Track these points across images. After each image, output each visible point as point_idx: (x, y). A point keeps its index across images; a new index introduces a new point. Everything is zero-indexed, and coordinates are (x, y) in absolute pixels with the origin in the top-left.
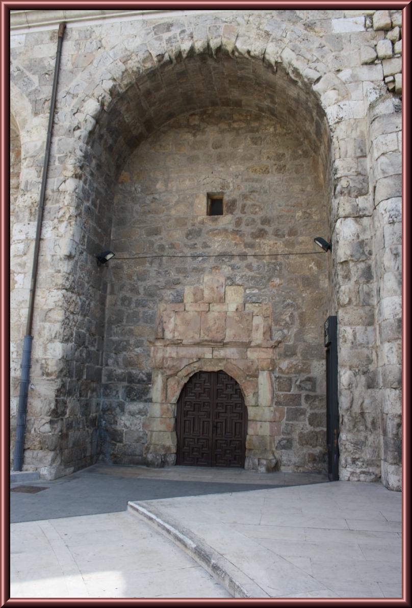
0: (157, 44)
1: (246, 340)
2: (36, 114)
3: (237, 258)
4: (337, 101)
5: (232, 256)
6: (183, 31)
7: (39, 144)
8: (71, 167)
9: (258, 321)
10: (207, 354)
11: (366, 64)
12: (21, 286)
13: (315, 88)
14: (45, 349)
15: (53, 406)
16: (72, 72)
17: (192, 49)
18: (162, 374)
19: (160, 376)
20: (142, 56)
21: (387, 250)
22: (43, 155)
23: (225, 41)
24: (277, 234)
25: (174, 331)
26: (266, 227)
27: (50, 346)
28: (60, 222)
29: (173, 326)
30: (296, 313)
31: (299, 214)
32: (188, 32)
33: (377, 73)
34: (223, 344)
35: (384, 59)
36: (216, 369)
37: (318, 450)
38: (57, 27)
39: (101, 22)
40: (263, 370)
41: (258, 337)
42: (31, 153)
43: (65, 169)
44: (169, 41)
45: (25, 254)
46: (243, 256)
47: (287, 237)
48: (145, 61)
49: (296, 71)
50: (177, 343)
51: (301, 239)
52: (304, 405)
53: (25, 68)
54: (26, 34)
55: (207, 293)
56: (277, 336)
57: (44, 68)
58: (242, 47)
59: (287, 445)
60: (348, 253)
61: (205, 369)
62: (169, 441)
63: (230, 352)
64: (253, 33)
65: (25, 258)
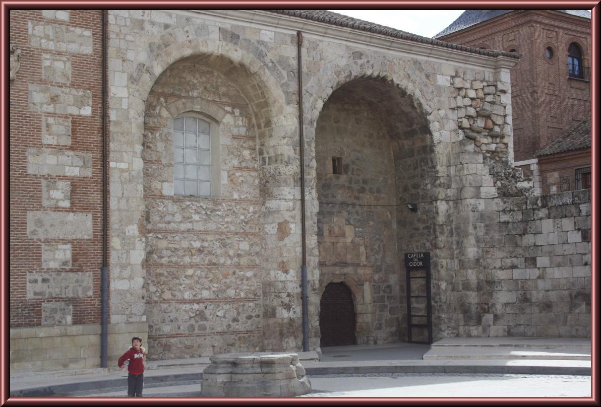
0: (355, 67)
2: (288, 104)
3: (351, 206)
5: (348, 205)
6: (368, 61)
7: (294, 128)
9: (362, 249)
10: (338, 271)
11: (452, 109)
12: (294, 232)
13: (430, 118)
16: (307, 74)
20: (347, 73)
21: (471, 224)
22: (297, 138)
23: (389, 75)
24: (371, 191)
26: (365, 186)
27: (315, 271)
28: (312, 188)
30: (381, 245)
31: (381, 178)
32: (371, 63)
33: (453, 116)
34: (345, 264)
36: (340, 281)
37: (394, 329)
39: (321, 38)
40: (366, 281)
41: (363, 259)
42: (289, 134)
43: (311, 151)
44: (361, 66)
45: (294, 210)
46: (354, 205)
47: (375, 194)
48: (346, 77)
49: (420, 105)
51: (383, 195)
52: (387, 303)
53: (277, 62)
54: (274, 32)
55: (336, 229)
57: (289, 65)
58: (396, 81)
59: (379, 328)
60: (444, 220)
61: (334, 281)
63: (349, 270)
64: (402, 73)
65: (294, 212)
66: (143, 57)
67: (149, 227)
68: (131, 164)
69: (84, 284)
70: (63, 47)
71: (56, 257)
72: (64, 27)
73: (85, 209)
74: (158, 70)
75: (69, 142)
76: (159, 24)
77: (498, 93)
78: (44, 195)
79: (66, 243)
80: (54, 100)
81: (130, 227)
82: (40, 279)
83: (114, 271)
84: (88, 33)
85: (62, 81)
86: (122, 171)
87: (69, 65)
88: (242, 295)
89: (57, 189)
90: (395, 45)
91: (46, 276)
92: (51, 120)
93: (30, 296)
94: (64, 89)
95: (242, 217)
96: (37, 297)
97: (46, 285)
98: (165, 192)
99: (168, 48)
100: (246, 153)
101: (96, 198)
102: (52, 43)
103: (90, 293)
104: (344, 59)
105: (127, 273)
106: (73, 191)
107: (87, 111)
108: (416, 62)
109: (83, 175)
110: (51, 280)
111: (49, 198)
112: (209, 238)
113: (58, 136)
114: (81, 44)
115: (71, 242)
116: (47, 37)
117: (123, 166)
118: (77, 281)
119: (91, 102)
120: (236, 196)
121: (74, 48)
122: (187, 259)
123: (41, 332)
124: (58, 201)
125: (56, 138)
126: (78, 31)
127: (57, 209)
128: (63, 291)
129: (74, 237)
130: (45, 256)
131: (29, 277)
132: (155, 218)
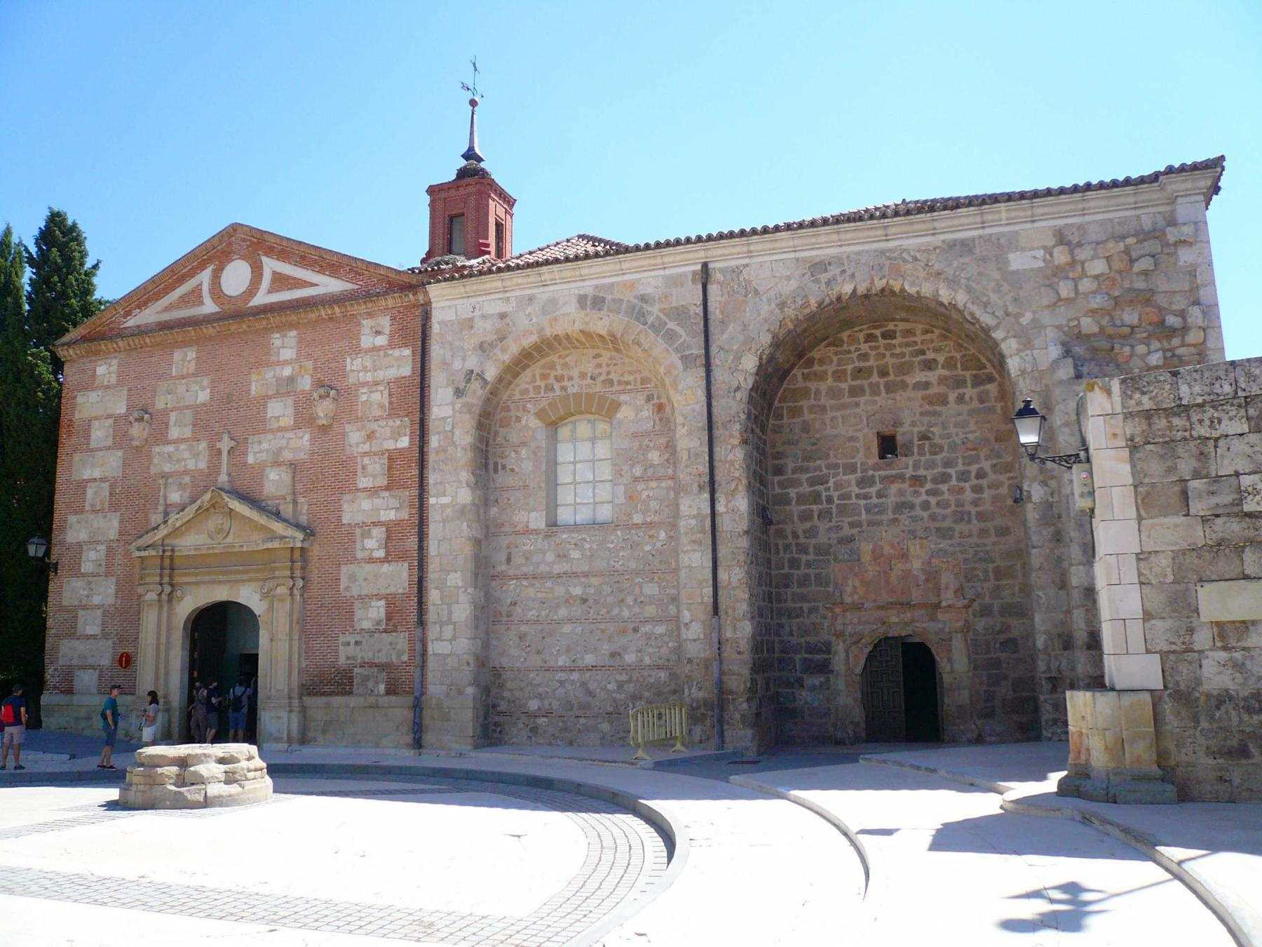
0: (815, 287)
1: (934, 600)
4: (1019, 351)
6: (843, 272)
8: (737, 434)
13: (998, 335)
14: (735, 629)
15: (749, 685)
17: (855, 290)
18: (844, 642)
19: (841, 644)
25: (851, 595)
29: (851, 590)
32: (849, 272)
35: (1068, 300)
38: (699, 267)
44: (828, 283)
49: (972, 314)
50: (858, 607)
56: (970, 594)
62: (858, 714)
66: (472, 363)
67: (511, 572)
68: (454, 497)
69: (399, 647)
70: (380, 375)
71: (370, 616)
72: (382, 353)
73: (401, 557)
74: (491, 373)
75: (383, 481)
76: (492, 315)
77: (1172, 249)
78: (358, 545)
79: (380, 599)
80: (370, 437)
81: (452, 575)
82: (352, 642)
83: (432, 632)
84: (407, 352)
85: (378, 413)
86: (444, 506)
87: (386, 393)
88: (647, 660)
89: (370, 537)
90: (893, 230)
91: (359, 638)
92: (366, 460)
93: (342, 660)
94: (381, 423)
95: (648, 548)
96: (349, 662)
97: (358, 648)
98: (532, 526)
99: (504, 342)
100: (654, 457)
101: (412, 542)
102: (369, 374)
103: (405, 658)
104: (792, 281)
105: (448, 631)
106: (388, 538)
107: (404, 442)
108: (952, 245)
109: (398, 518)
110: (364, 643)
111: (364, 549)
112: (595, 581)
113: (374, 476)
114: (399, 366)
115: (386, 597)
116: (365, 369)
117: (445, 500)
118: (391, 644)
119: (408, 431)
120: (637, 519)
121: (392, 373)
122: (563, 612)
123: (353, 701)
124: (372, 550)
125: (371, 479)
126: (397, 352)
127: (371, 560)
128: (376, 655)
129: (388, 592)
130: (358, 614)
131: (342, 639)
132: (518, 559)
